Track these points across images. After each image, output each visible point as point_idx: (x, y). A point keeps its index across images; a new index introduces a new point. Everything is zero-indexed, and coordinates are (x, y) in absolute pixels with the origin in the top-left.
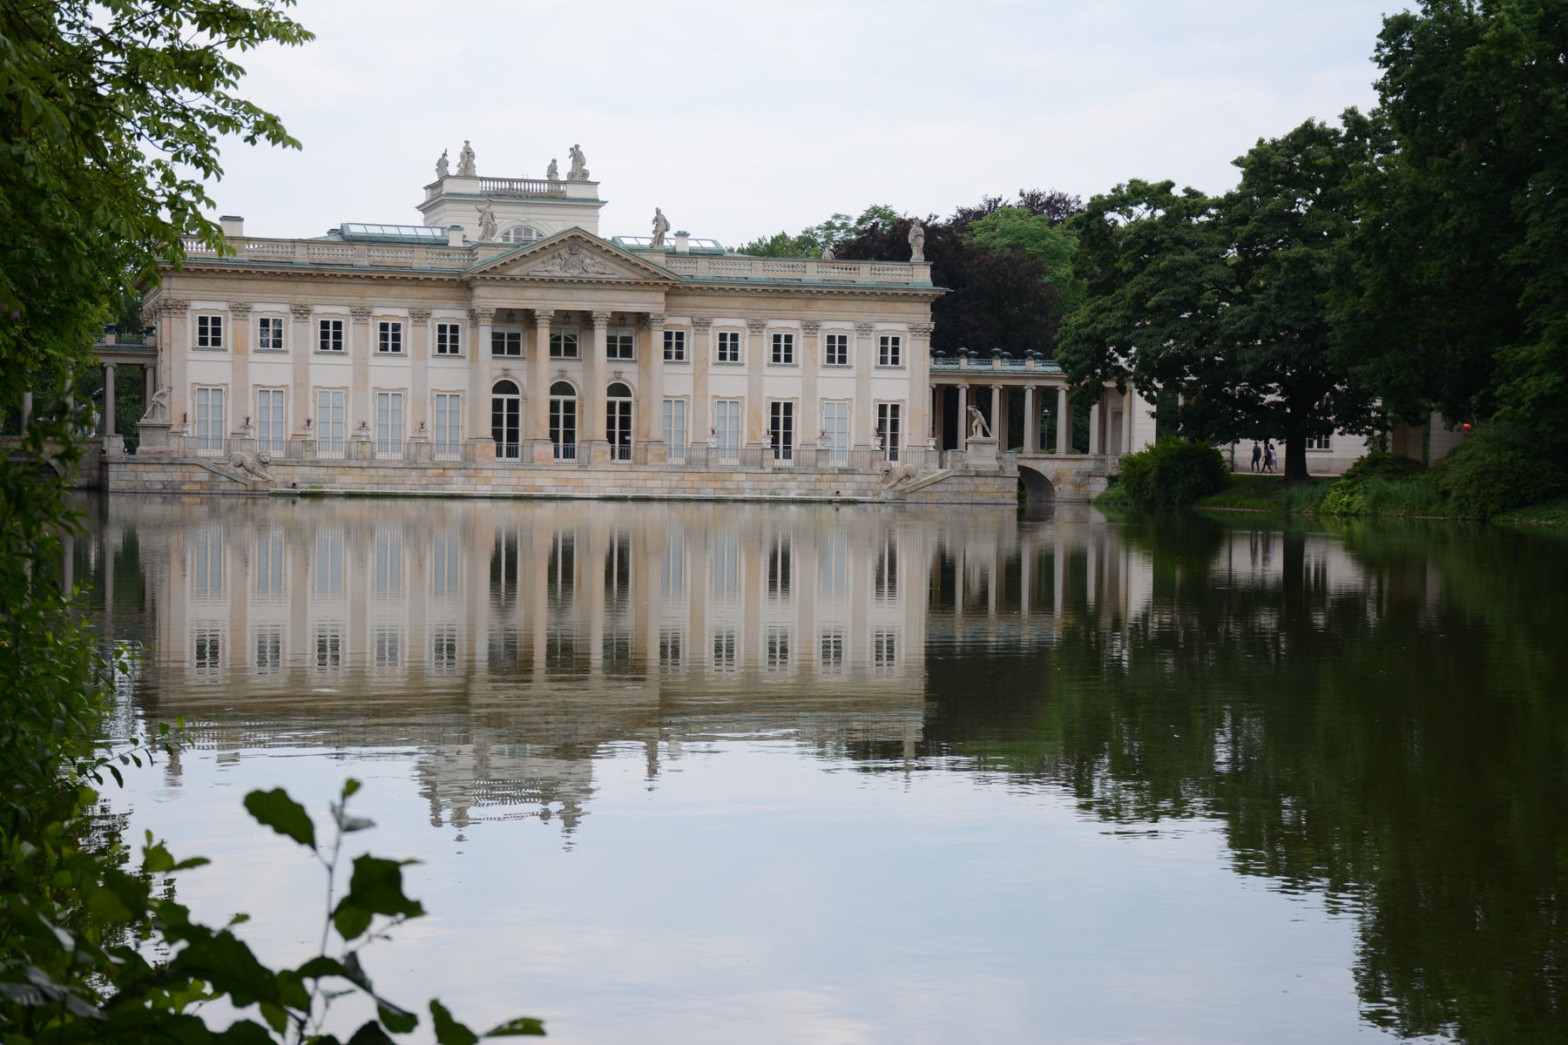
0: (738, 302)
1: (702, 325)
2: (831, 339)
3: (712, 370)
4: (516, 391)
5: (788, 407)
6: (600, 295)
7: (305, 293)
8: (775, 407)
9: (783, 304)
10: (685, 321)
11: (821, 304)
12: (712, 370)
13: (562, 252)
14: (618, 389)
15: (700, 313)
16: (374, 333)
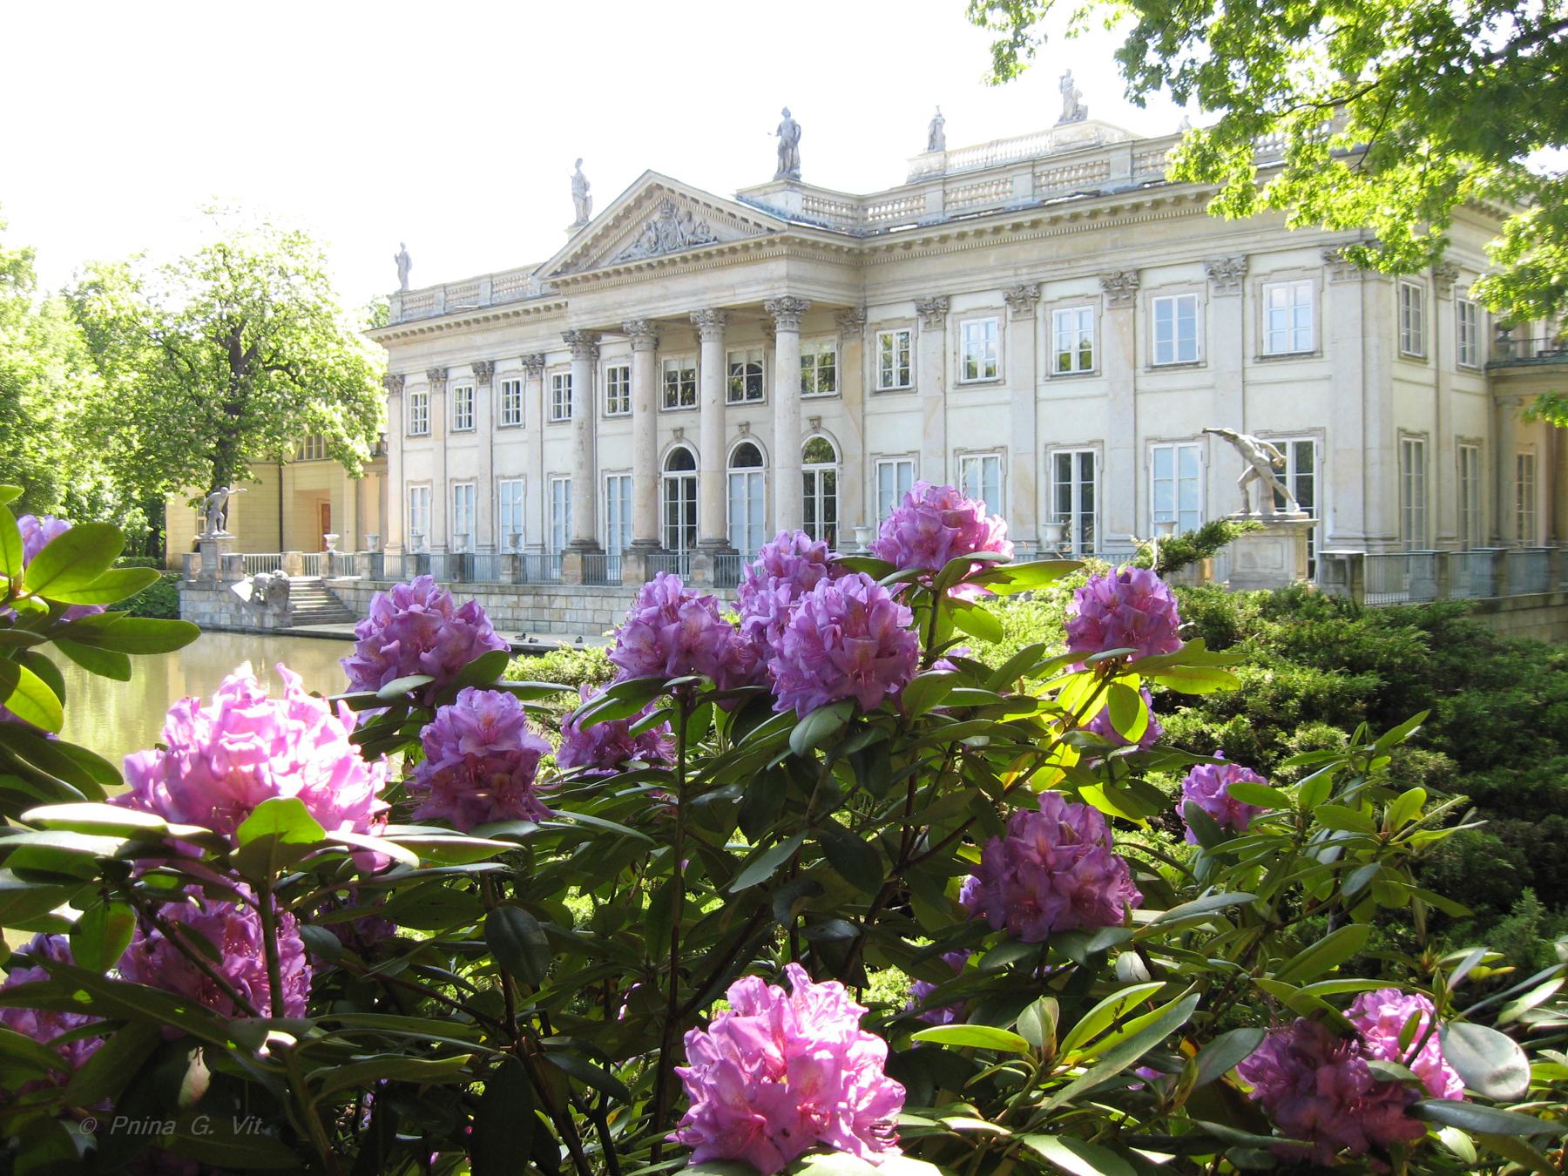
0: (993, 257)
1: (934, 311)
2: (1164, 308)
3: (954, 397)
4: (692, 466)
5: (1087, 460)
6: (701, 281)
7: (484, 345)
8: (1064, 462)
9: (1066, 247)
10: (909, 311)
11: (1138, 234)
12: (954, 397)
13: (656, 217)
14: (820, 451)
15: (929, 290)
16: (549, 389)
